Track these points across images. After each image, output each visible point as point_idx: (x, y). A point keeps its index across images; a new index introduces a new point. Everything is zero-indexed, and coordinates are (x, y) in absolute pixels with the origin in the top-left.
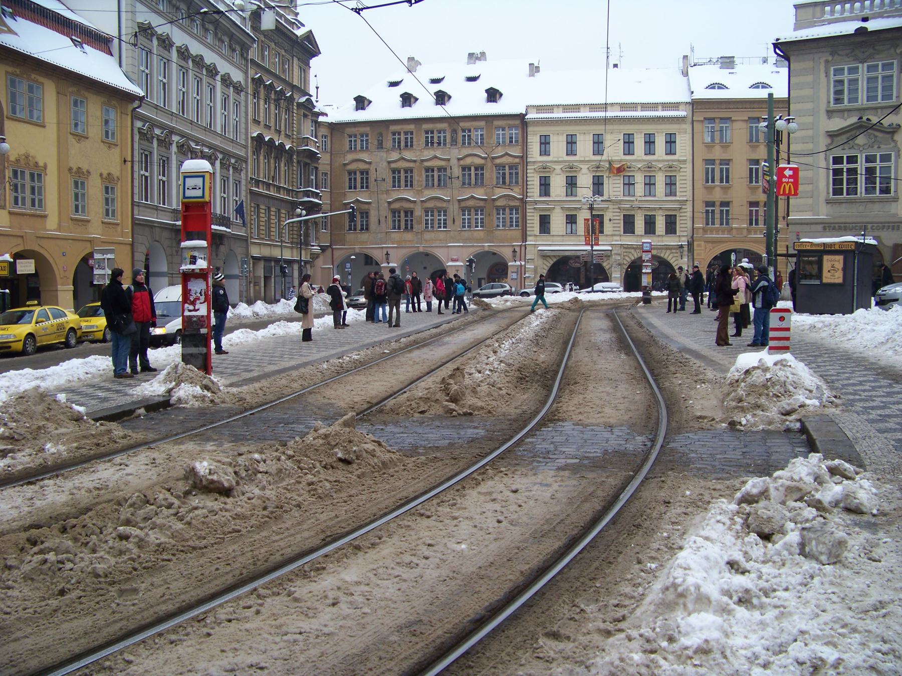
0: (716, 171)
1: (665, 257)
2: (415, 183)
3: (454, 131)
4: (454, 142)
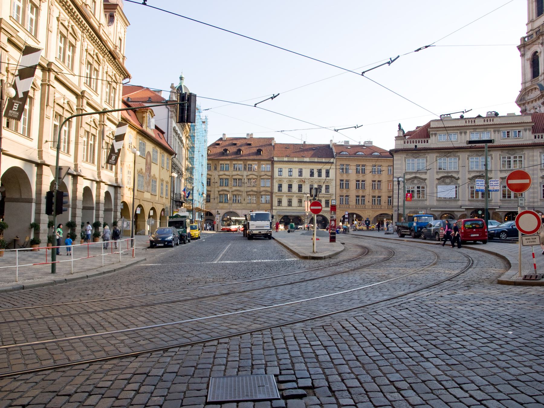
2: (229, 184)
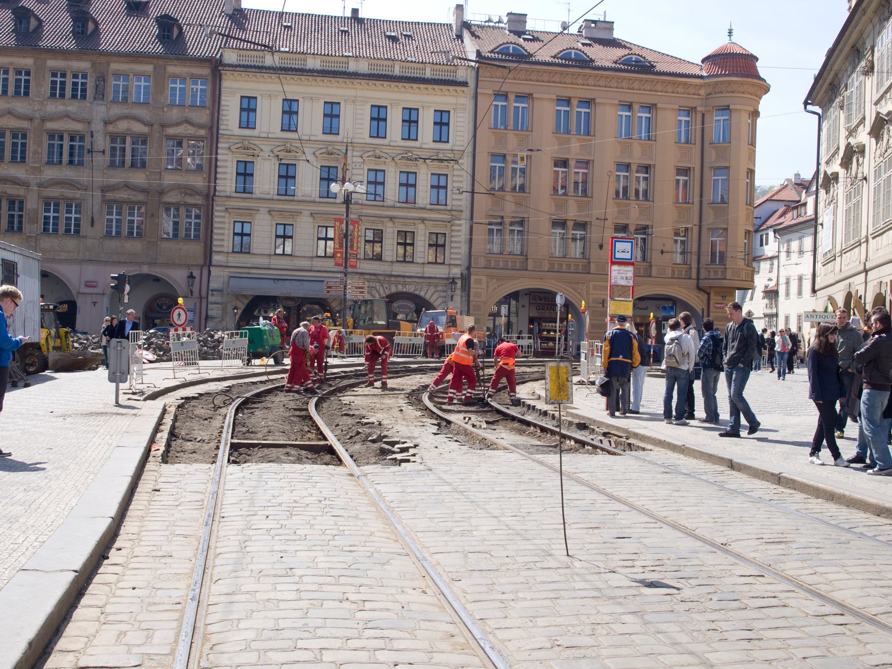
1: (427, 297)
2: (29, 155)
4: (100, 94)
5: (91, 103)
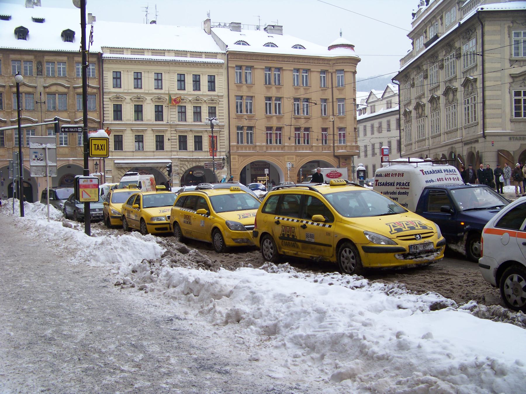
0: (242, 105)
3: (40, 63)
5: (36, 77)
